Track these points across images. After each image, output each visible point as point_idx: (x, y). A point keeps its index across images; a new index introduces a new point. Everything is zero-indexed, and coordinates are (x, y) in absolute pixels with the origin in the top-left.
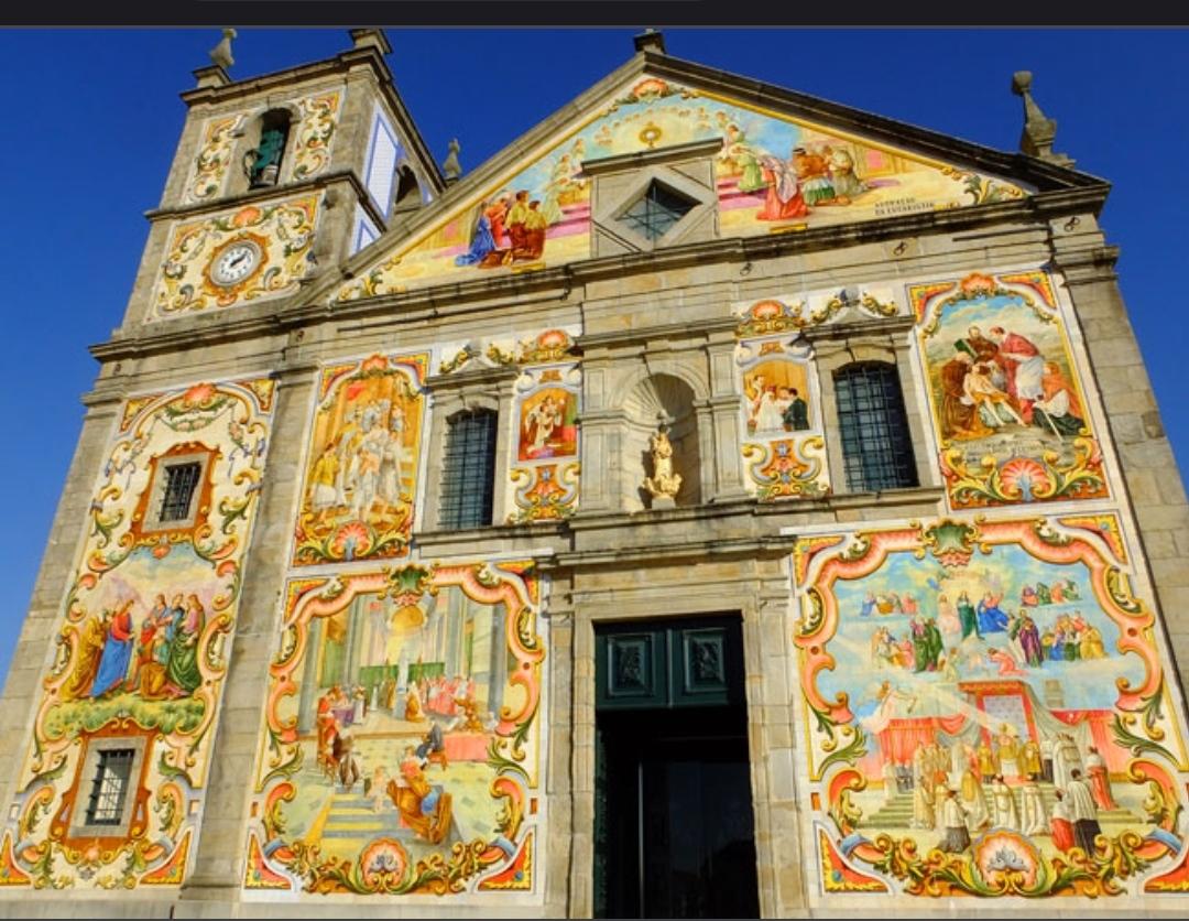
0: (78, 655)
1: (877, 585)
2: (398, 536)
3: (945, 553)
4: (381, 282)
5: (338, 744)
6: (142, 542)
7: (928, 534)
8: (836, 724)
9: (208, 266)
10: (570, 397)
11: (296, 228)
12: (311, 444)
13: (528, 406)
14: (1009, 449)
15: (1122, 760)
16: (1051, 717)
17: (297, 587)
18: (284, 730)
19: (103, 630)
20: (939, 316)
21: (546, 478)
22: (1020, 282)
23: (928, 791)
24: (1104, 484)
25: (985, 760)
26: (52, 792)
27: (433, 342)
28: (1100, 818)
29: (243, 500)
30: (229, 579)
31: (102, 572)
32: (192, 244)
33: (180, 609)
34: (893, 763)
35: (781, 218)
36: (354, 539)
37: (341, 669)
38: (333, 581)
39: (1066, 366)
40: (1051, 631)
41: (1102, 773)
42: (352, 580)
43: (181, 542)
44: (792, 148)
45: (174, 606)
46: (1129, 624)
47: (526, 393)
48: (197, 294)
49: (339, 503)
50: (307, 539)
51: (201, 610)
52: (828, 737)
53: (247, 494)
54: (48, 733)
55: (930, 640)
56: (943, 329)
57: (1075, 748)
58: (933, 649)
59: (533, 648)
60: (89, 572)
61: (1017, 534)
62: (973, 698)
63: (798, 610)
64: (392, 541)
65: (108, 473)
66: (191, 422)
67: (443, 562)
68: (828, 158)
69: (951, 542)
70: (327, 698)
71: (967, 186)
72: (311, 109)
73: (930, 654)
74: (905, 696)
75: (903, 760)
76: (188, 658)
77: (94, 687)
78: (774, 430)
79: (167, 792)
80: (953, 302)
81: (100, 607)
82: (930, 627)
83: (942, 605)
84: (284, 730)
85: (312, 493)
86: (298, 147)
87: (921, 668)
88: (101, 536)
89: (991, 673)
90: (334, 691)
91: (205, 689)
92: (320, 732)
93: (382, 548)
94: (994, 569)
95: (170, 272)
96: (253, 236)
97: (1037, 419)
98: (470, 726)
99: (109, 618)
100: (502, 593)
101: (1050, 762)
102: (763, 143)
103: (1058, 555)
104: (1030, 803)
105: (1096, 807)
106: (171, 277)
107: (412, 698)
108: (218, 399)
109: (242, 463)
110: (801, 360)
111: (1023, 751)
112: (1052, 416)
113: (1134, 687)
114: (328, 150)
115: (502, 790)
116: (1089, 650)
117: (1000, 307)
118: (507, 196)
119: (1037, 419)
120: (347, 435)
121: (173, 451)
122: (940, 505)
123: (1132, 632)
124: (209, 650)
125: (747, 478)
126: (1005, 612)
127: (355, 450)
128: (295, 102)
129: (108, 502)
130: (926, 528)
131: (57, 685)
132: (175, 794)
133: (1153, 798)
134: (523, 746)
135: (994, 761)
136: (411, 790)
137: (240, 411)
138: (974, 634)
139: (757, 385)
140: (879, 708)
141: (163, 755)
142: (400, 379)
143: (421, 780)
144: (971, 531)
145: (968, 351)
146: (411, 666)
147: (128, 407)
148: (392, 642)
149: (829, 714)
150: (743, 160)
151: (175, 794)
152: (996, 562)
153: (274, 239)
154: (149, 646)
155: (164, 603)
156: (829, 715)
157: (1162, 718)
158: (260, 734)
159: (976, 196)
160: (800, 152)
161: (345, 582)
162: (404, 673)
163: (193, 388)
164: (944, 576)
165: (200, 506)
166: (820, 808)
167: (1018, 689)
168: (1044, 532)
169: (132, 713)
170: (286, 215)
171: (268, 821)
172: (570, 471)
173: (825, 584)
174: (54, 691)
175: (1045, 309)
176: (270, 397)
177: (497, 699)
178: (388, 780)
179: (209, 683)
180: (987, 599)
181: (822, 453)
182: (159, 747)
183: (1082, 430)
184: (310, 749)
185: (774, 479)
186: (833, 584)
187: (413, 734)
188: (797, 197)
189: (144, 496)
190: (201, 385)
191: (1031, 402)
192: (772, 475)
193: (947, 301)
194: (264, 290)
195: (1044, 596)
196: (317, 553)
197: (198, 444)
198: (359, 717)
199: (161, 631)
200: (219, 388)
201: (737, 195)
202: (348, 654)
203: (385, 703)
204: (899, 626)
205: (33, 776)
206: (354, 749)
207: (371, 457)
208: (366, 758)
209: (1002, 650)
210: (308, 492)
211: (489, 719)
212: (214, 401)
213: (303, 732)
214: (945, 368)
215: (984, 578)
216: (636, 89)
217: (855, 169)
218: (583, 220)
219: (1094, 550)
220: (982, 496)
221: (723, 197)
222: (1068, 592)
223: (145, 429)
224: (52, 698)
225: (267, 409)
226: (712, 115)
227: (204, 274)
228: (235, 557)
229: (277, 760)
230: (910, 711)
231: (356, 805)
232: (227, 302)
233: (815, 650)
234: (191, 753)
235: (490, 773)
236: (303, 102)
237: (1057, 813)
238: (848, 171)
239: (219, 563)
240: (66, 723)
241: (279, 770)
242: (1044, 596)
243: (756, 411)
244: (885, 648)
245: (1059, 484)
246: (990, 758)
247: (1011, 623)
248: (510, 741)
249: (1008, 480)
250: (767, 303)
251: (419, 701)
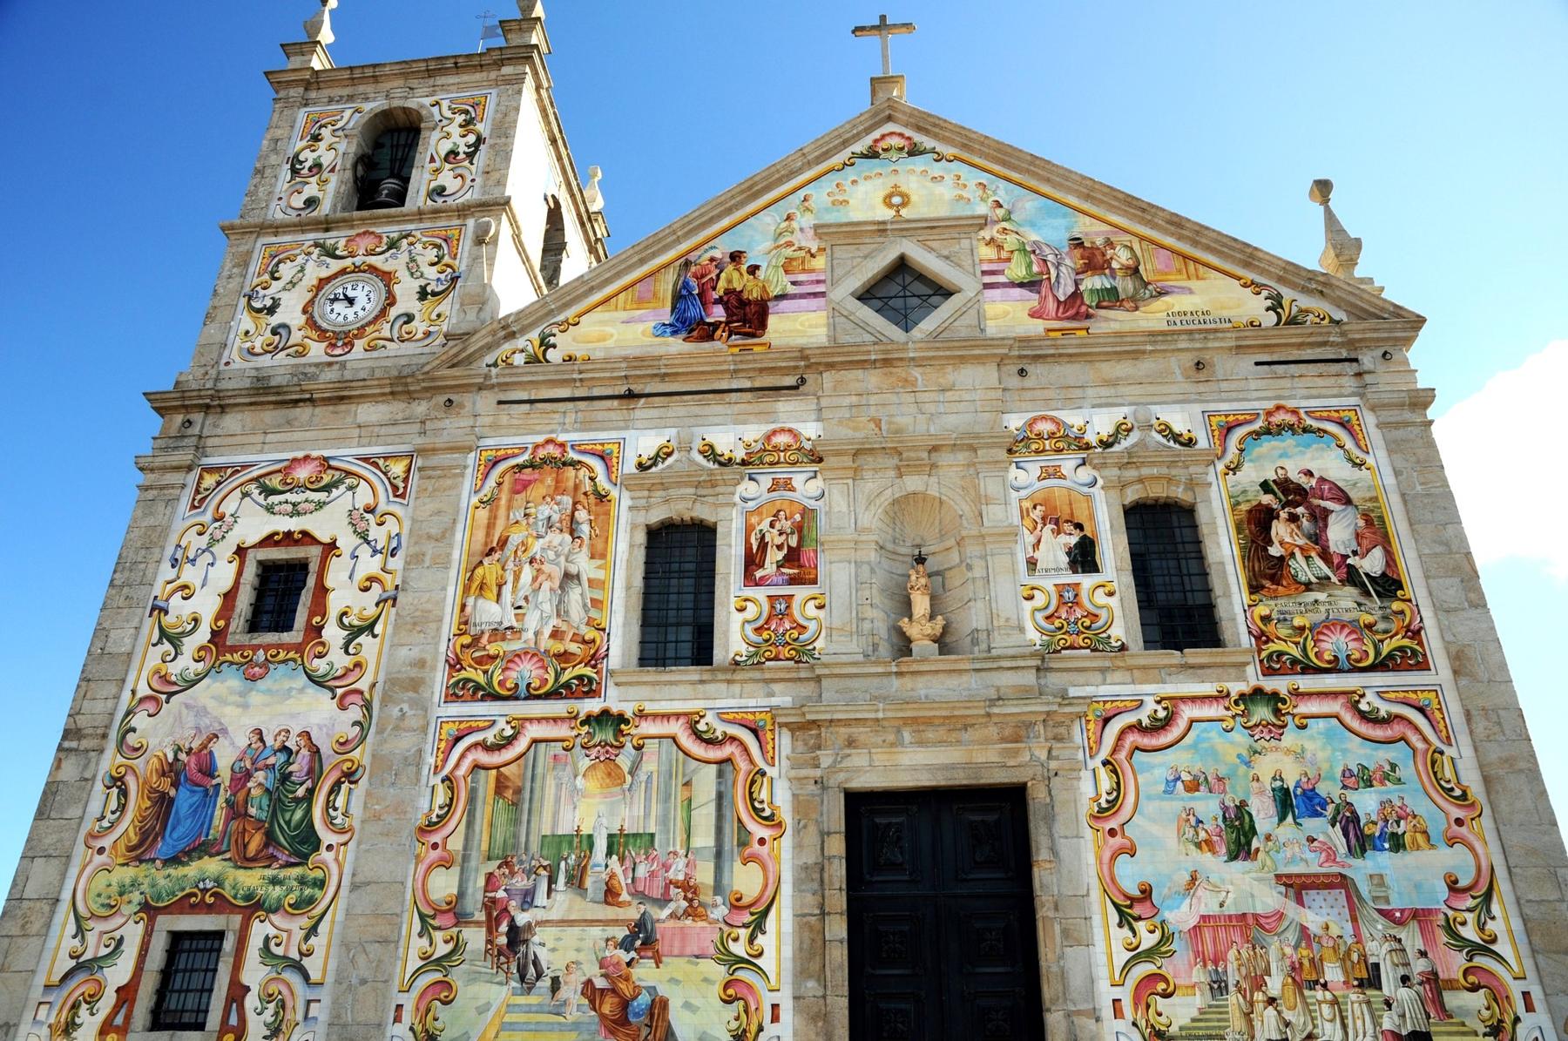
0: (137, 802)
1: (1181, 759)
2: (588, 671)
3: (1256, 726)
4: (554, 346)
5: (513, 928)
6: (228, 657)
7: (1236, 703)
8: (1139, 919)
9: (311, 302)
10: (806, 512)
11: (433, 264)
12: (466, 547)
13: (754, 520)
14: (1322, 609)
15: (1454, 964)
16: (1376, 915)
17: (451, 729)
18: (438, 912)
19: (173, 771)
20: (1242, 450)
21: (780, 610)
22: (1329, 420)
23: (1244, 997)
24: (1425, 655)
25: (1306, 962)
26: (101, 986)
27: (627, 428)
28: (1433, 1029)
29: (372, 611)
30: (355, 713)
31: (170, 695)
32: (287, 271)
33: (284, 749)
34: (1205, 965)
35: (1058, 318)
36: (527, 672)
37: (516, 836)
38: (501, 723)
39: (1381, 518)
40: (1374, 818)
41: (1432, 979)
42: (527, 724)
43: (284, 661)
44: (1067, 236)
45: (277, 745)
46: (1457, 813)
47: (751, 504)
48: (296, 337)
49: (506, 624)
50: (462, 668)
51: (316, 752)
52: (1130, 934)
53: (377, 605)
54: (94, 907)
55: (1242, 824)
56: (1246, 467)
57: (1404, 950)
58: (1245, 835)
59: (771, 820)
60: (150, 692)
61: (1335, 706)
62: (1291, 892)
63: (1090, 786)
64: (580, 678)
65: (175, 563)
66: (294, 505)
67: (649, 708)
68: (1110, 252)
69: (1262, 713)
70: (497, 873)
71: (1269, 303)
72: (448, 114)
73: (1243, 839)
74: (1216, 889)
75: (1216, 963)
76: (299, 814)
77: (162, 848)
78: (1058, 569)
79: (273, 988)
80: (1257, 435)
81: (169, 740)
82: (1241, 807)
83: (1255, 784)
84: (438, 912)
85: (468, 609)
86: (432, 160)
87: (1233, 857)
88: (167, 646)
89: (1312, 864)
90: (506, 864)
91: (325, 855)
92: (489, 915)
93: (567, 685)
94: (1309, 746)
95: (257, 305)
96: (372, 269)
97: (1352, 577)
98: (694, 911)
99: (183, 756)
100: (728, 750)
101: (1377, 966)
102: (1033, 225)
103: (1378, 732)
104: (1358, 1013)
105: (1428, 1017)
106: (259, 311)
107: (612, 876)
108: (330, 477)
109: (370, 565)
110: (1086, 489)
111: (1348, 952)
112: (1367, 575)
113: (1463, 883)
114: (473, 168)
115: (733, 993)
116: (1414, 840)
117: (1308, 446)
118: (717, 254)
119: (1352, 577)
120: (515, 538)
121: (269, 541)
122: (1250, 670)
123: (1459, 822)
124: (329, 805)
125: (1029, 626)
126: (1324, 795)
127: (525, 558)
129: (176, 600)
130: (1234, 696)
131: (107, 842)
132: (285, 991)
133: (1488, 1008)
134: (761, 940)
135: (1317, 965)
136: (614, 991)
137: (364, 496)
138: (1290, 818)
139: (1037, 514)
140: (1188, 901)
141: (267, 940)
142: (583, 472)
143: (627, 979)
144: (1284, 701)
145: (1275, 494)
146: (610, 836)
147: (201, 478)
148: (580, 805)
149: (1130, 907)
150: (1010, 242)
151: (285, 991)
152: (1312, 738)
153: (403, 274)
154: (241, 796)
155: (261, 740)
156: (1132, 908)
157: (1493, 918)
158: (406, 916)
159: (1278, 314)
160: (1077, 243)
161: (519, 725)
162: (601, 845)
163: (294, 460)
164: (1255, 752)
165: (311, 615)
166: (1122, 1017)
167: (1342, 882)
168: (1363, 706)
169: (219, 882)
170: (419, 246)
171: (418, 1028)
172: (811, 604)
173: (1122, 755)
174: (101, 851)
175: (1356, 452)
176: (406, 480)
177: (725, 881)
178: (584, 979)
179: (330, 848)
180: (1304, 780)
181: (1113, 602)
182: (259, 930)
183: (1399, 593)
184: (475, 938)
185: (1060, 629)
186: (1131, 755)
187: (615, 922)
188: (1076, 295)
189: (229, 597)
190: (307, 458)
191: (1346, 557)
192: (1057, 623)
193: (1250, 434)
194: (391, 340)
195: (1364, 778)
196: (478, 687)
197: (305, 533)
198: (541, 898)
199: (260, 776)
200: (332, 463)
201: (1004, 285)
202: (525, 818)
203: (576, 881)
204: (1209, 807)
205: (73, 963)
206: (536, 939)
207: (546, 568)
208: (553, 950)
209: (1321, 838)
210: (463, 607)
211: (715, 906)
212: (326, 479)
213: (465, 915)
214: (1250, 512)
215: (1300, 755)
216: (876, 141)
217: (1141, 268)
218: (815, 295)
219: (1417, 729)
220: (1295, 661)
221: (987, 286)
222: (1389, 774)
223: (229, 507)
224: (99, 859)
225: (403, 496)
226: (972, 184)
228: (363, 685)
229: (430, 950)
230: (1221, 905)
231: (540, 1009)
232: (338, 351)
233: (1112, 832)
234: (307, 938)
235: (719, 972)
237: (1387, 1024)
238: (1134, 271)
239: (339, 691)
240: (121, 895)
241: (430, 962)
242: (1364, 778)
243: (1036, 545)
244: (1192, 831)
245: (1378, 653)
246: (1312, 961)
247: (1331, 808)
248: (744, 933)
249: (1323, 645)
250: (1044, 418)
251: (623, 880)
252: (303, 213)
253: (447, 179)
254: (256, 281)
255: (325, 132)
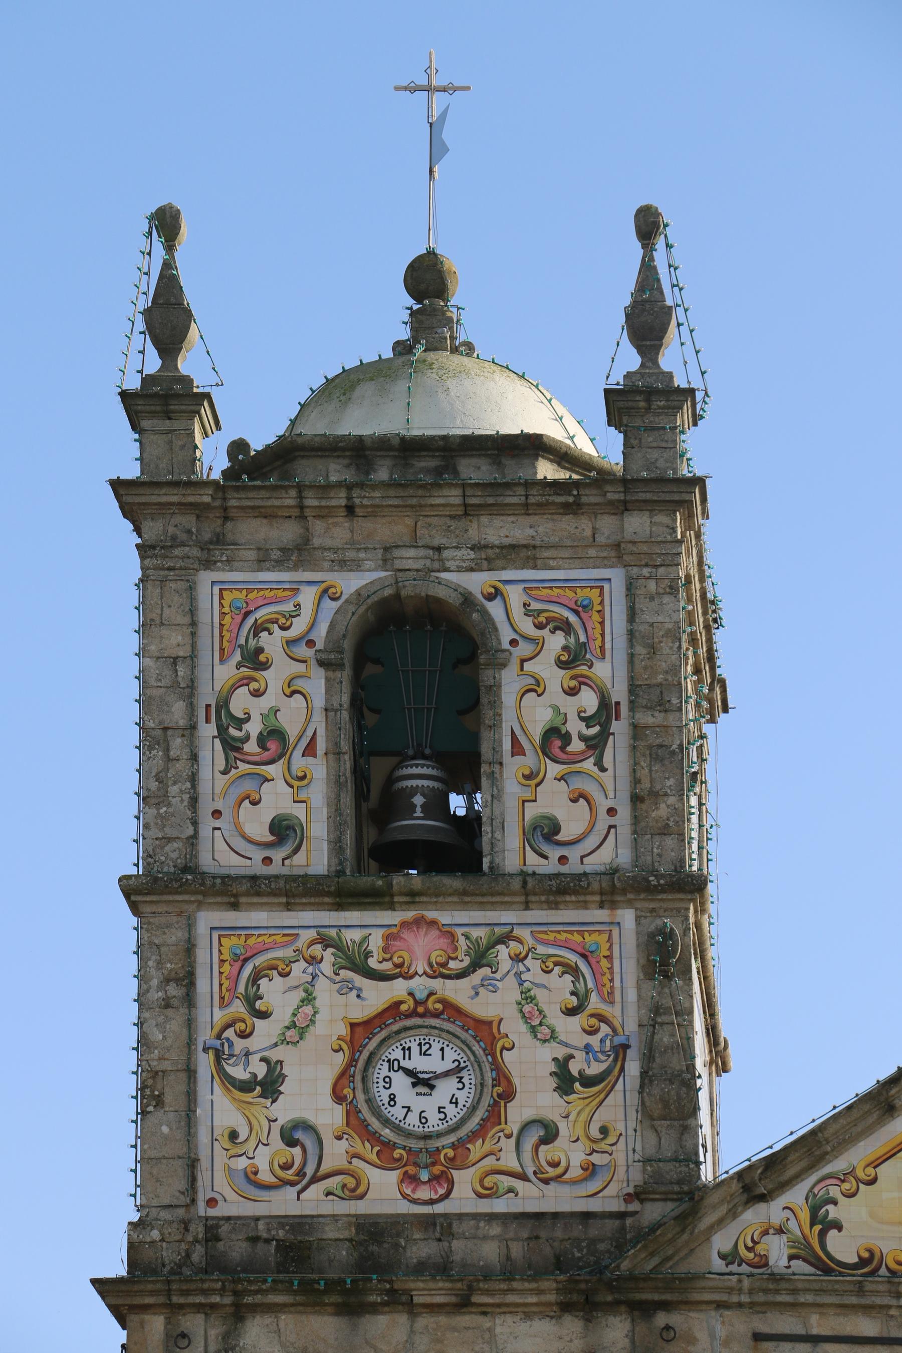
9: (344, 1075)
11: (571, 1012)
32: (277, 995)
48: (336, 1153)
72: (527, 626)
95: (239, 1073)
96: (451, 1010)
106: (245, 1087)
114: (607, 778)
128: (477, 582)
153: (514, 1029)
227: (338, 1098)
232: (424, 1193)
236: (495, 594)
252: (278, 855)
253: (552, 800)
254: (220, 1016)
255: (272, 643)
